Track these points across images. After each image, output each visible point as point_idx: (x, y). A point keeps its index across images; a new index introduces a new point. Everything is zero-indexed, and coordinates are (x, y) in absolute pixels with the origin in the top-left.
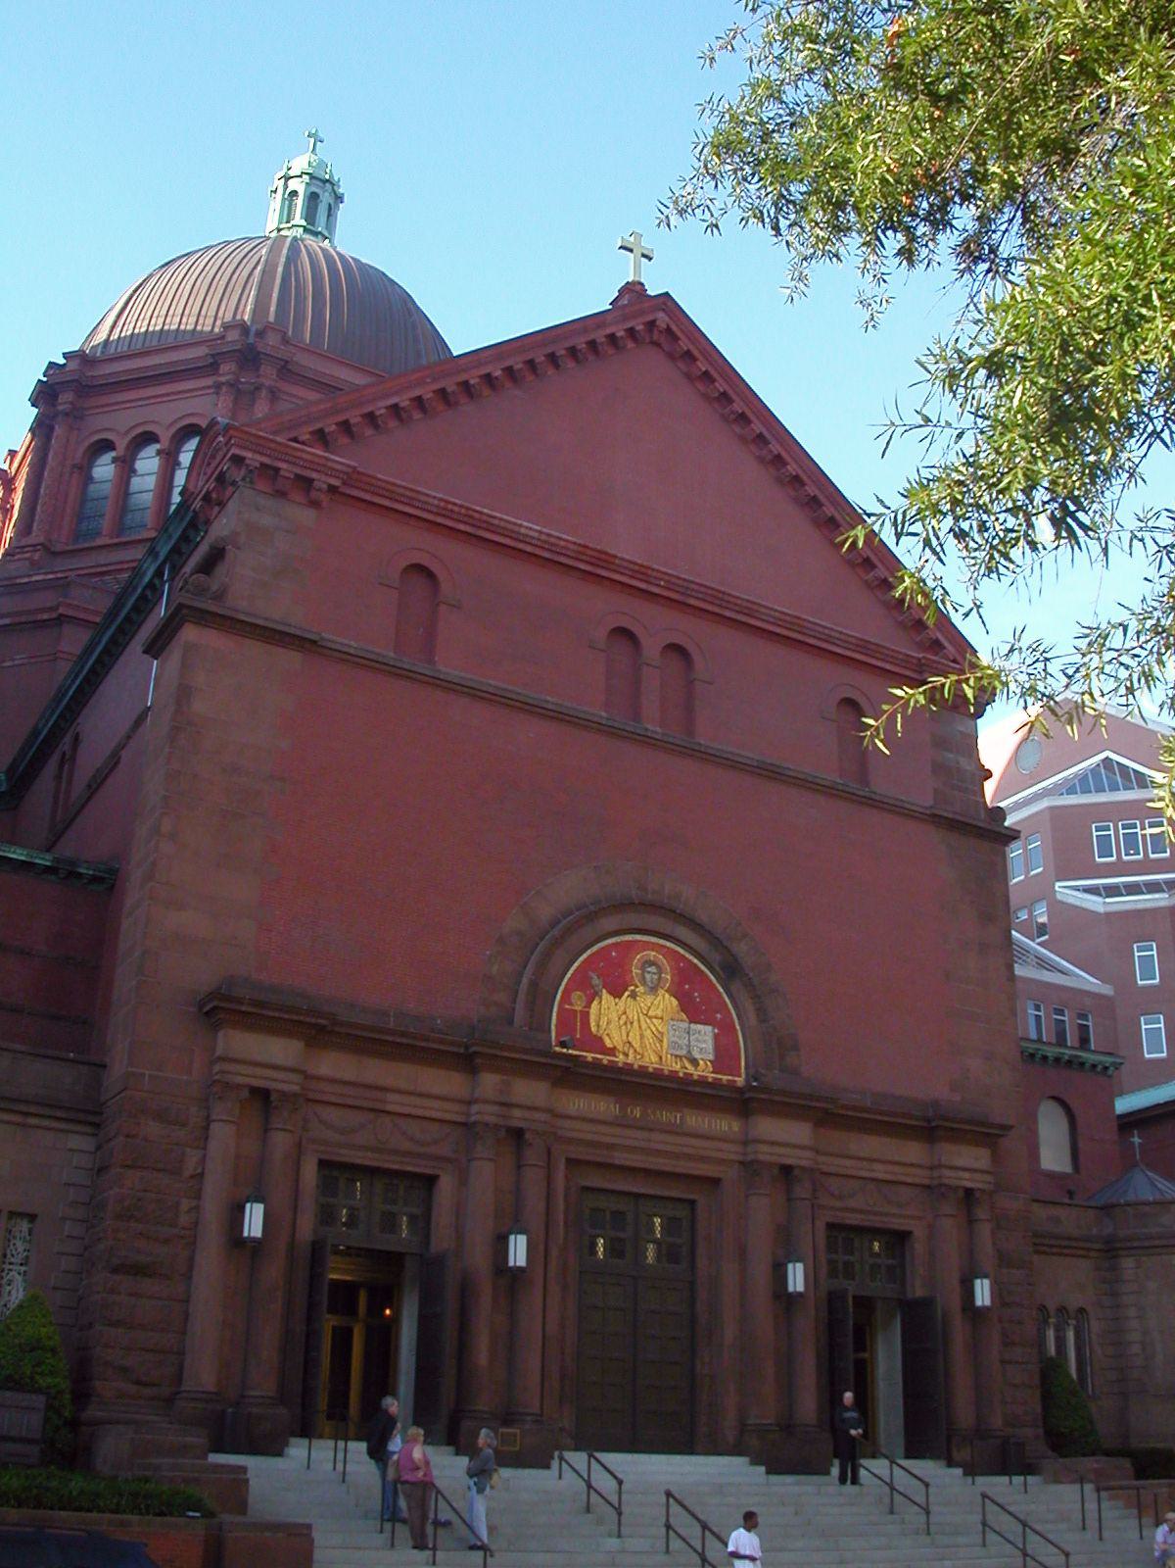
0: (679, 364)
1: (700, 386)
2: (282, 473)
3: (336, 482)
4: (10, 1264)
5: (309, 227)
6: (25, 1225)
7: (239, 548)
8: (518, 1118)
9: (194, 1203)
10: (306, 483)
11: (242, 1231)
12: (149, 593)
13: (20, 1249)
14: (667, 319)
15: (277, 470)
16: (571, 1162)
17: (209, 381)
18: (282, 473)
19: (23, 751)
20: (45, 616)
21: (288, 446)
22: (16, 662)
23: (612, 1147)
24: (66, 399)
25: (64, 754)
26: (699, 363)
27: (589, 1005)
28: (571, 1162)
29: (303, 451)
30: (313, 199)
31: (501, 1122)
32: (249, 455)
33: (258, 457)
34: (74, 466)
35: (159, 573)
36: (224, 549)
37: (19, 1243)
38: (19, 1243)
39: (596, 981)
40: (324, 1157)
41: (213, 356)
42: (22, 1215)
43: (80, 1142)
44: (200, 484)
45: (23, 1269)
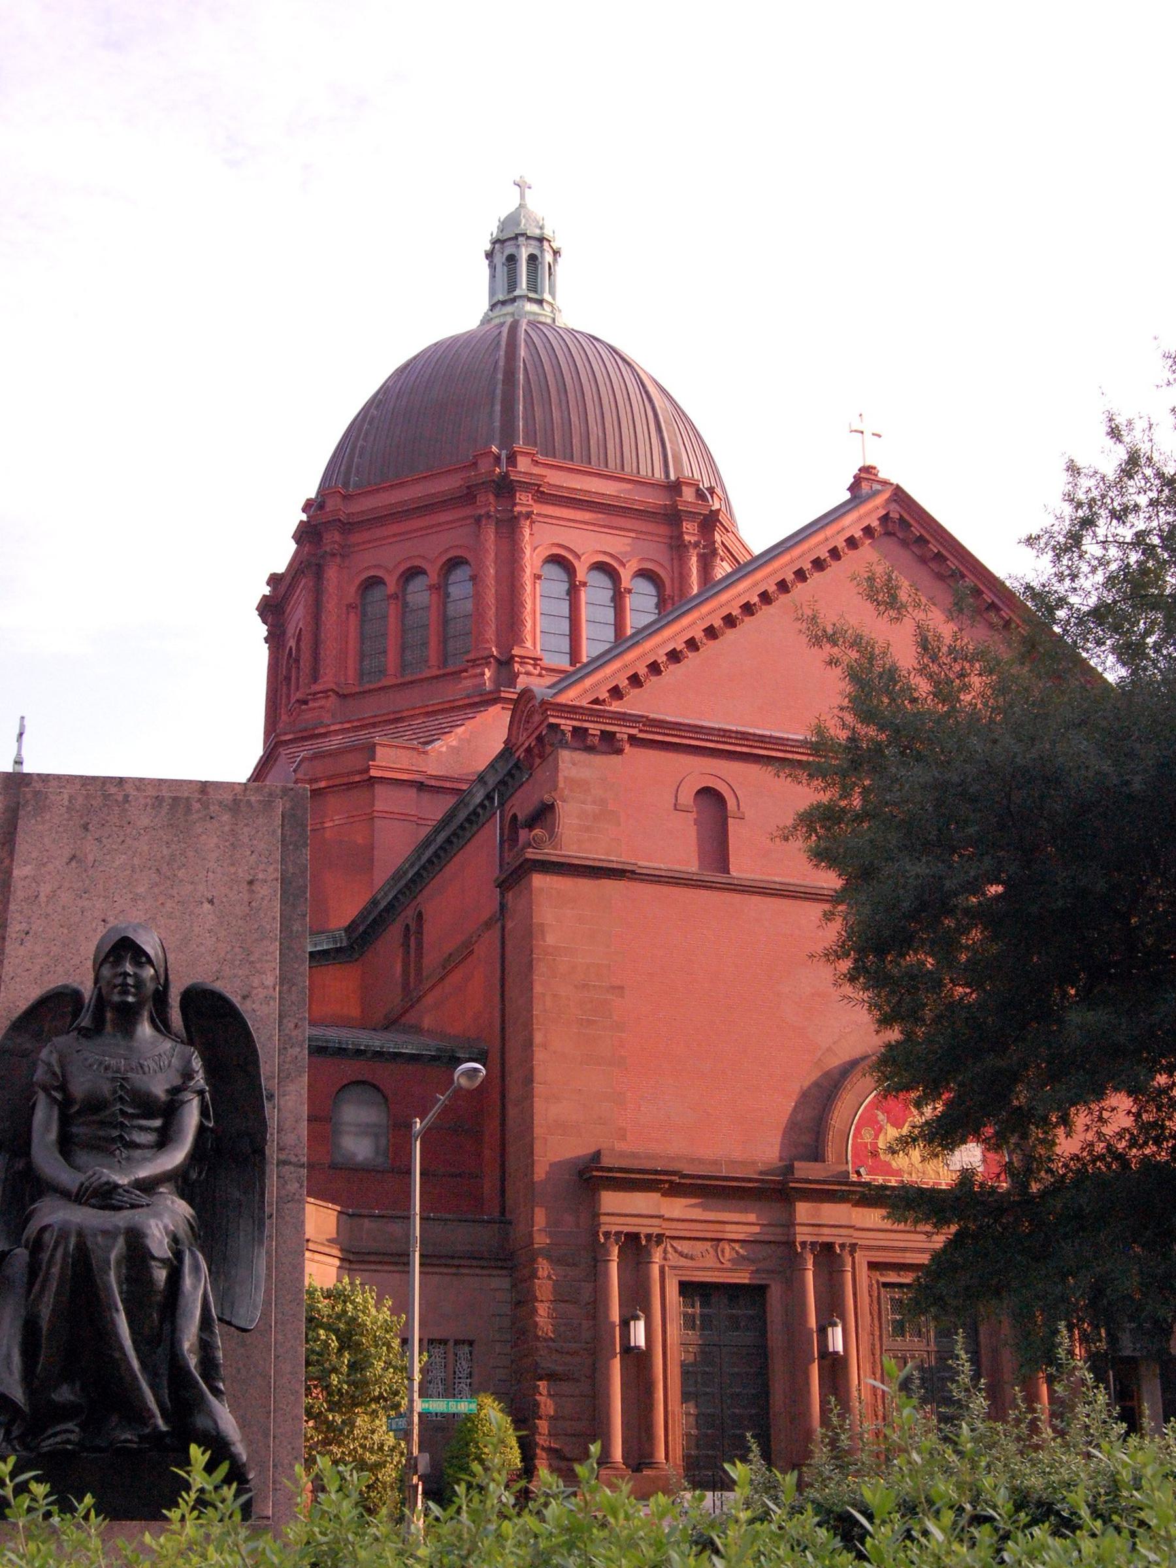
0: (915, 550)
1: (933, 565)
2: (591, 731)
3: (634, 731)
4: (460, 1378)
5: (531, 295)
6: (466, 1349)
7: (564, 801)
8: (827, 1235)
9: (591, 1323)
10: (608, 737)
11: (629, 1343)
12: (480, 810)
13: (465, 1367)
14: (898, 508)
15: (586, 730)
16: (873, 1266)
17: (468, 511)
18: (591, 731)
19: (363, 915)
20: (357, 778)
21: (592, 709)
22: (337, 822)
23: (904, 1250)
24: (332, 539)
25: (407, 927)
26: (931, 546)
27: (876, 1137)
28: (873, 1266)
29: (604, 711)
30: (532, 258)
31: (814, 1239)
32: (562, 721)
33: (568, 722)
34: (349, 606)
35: (489, 797)
36: (553, 804)
37: (464, 1363)
38: (464, 1363)
39: (881, 1117)
40: (684, 1279)
41: (468, 487)
42: (463, 1342)
43: (500, 1282)
44: (521, 739)
45: (469, 1381)
